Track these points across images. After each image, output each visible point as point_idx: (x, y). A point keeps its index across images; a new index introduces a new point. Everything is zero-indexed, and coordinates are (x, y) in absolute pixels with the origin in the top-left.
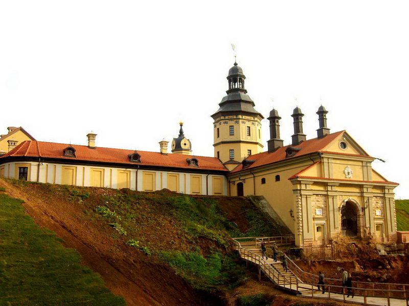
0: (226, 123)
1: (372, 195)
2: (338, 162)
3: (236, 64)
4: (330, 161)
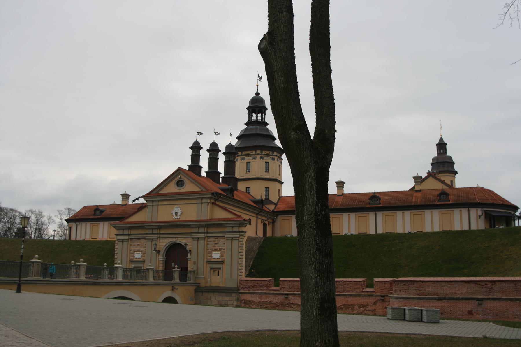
1: (203, 236)
2: (165, 203)
3: (257, 94)
4: (155, 203)
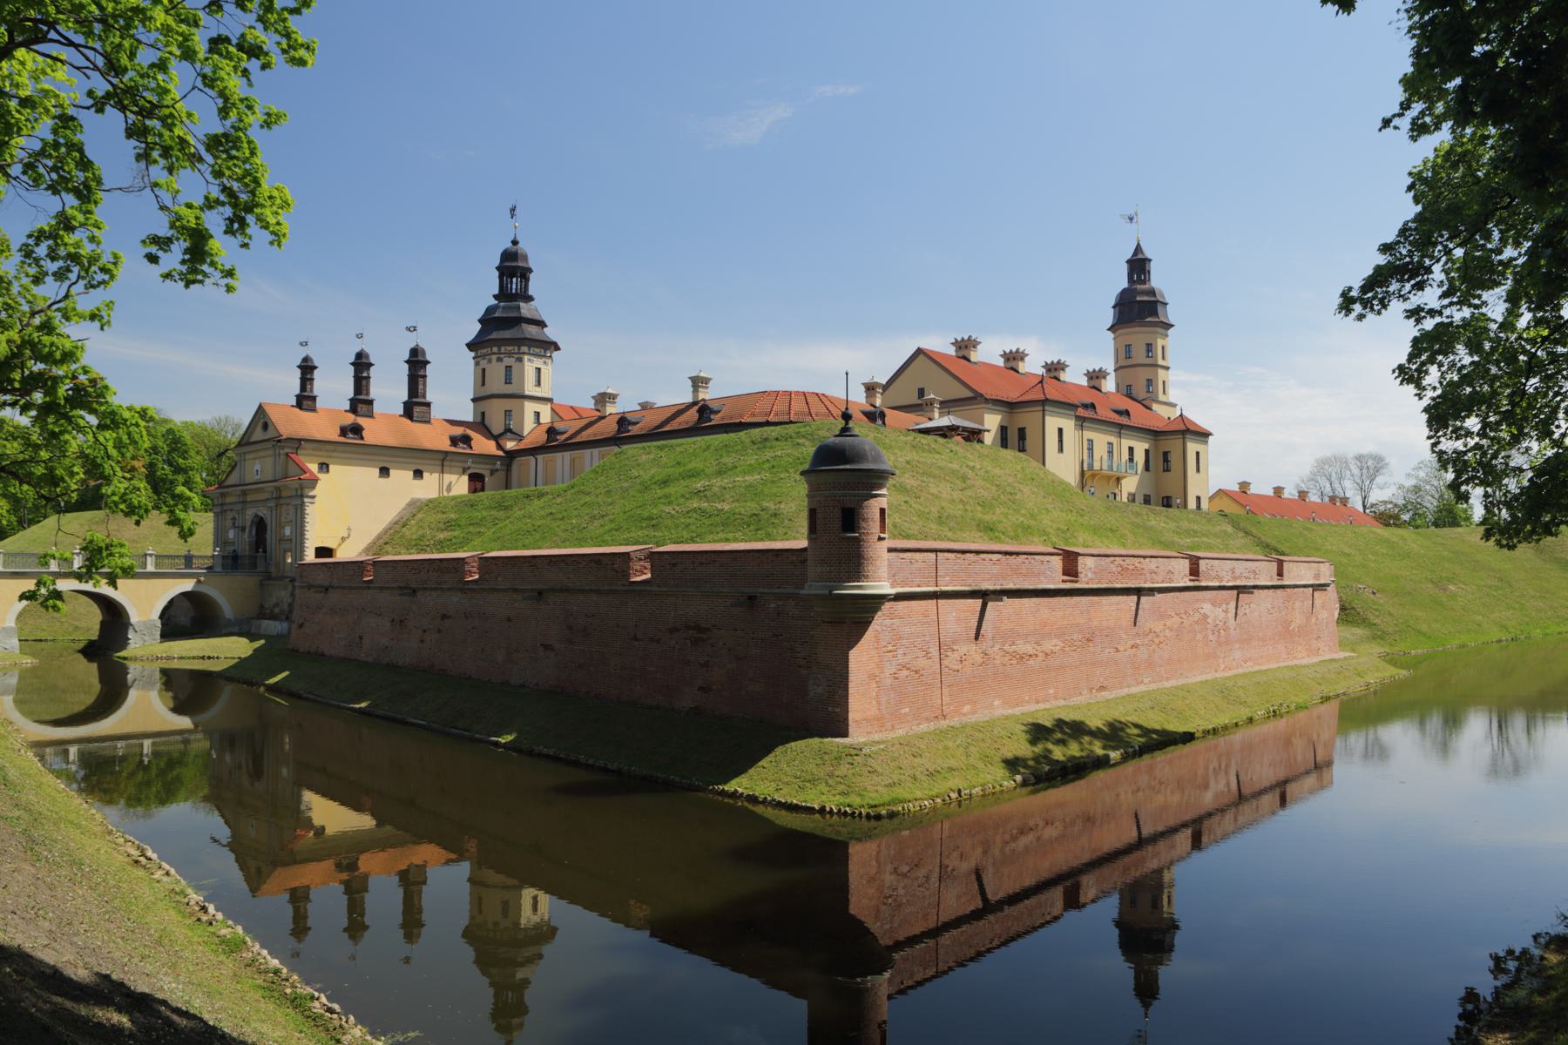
0: (499, 360)
3: (515, 242)
